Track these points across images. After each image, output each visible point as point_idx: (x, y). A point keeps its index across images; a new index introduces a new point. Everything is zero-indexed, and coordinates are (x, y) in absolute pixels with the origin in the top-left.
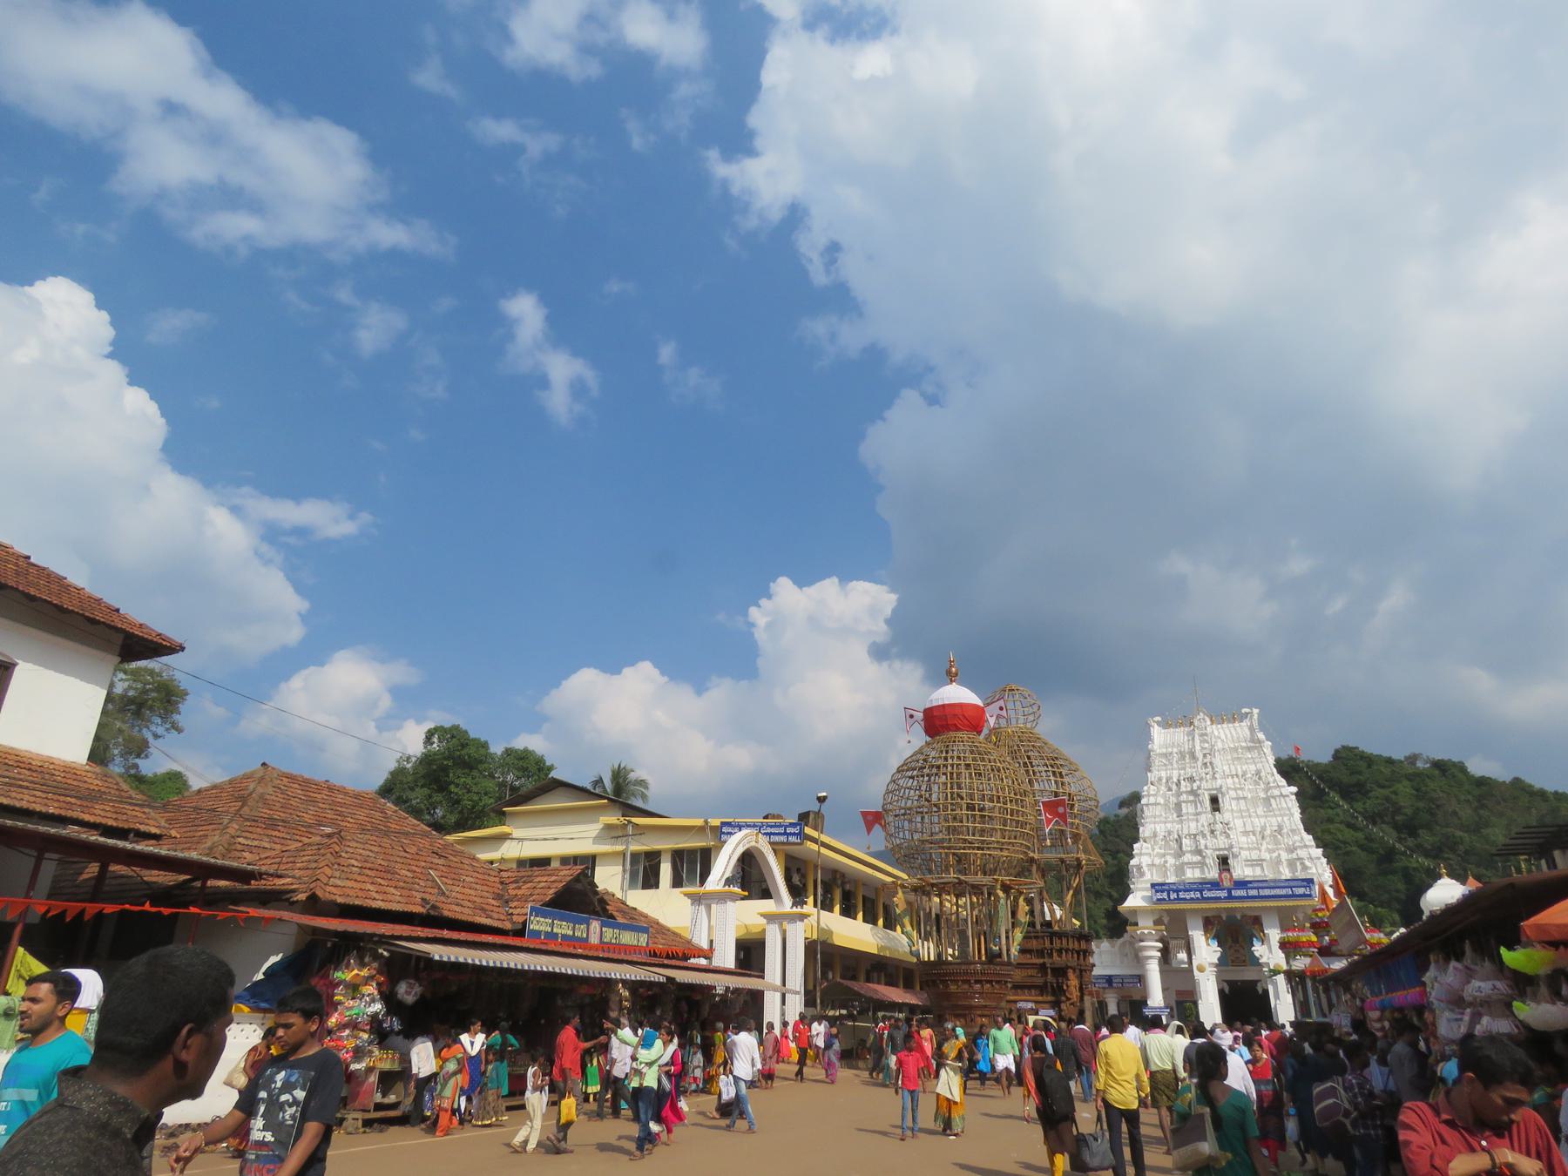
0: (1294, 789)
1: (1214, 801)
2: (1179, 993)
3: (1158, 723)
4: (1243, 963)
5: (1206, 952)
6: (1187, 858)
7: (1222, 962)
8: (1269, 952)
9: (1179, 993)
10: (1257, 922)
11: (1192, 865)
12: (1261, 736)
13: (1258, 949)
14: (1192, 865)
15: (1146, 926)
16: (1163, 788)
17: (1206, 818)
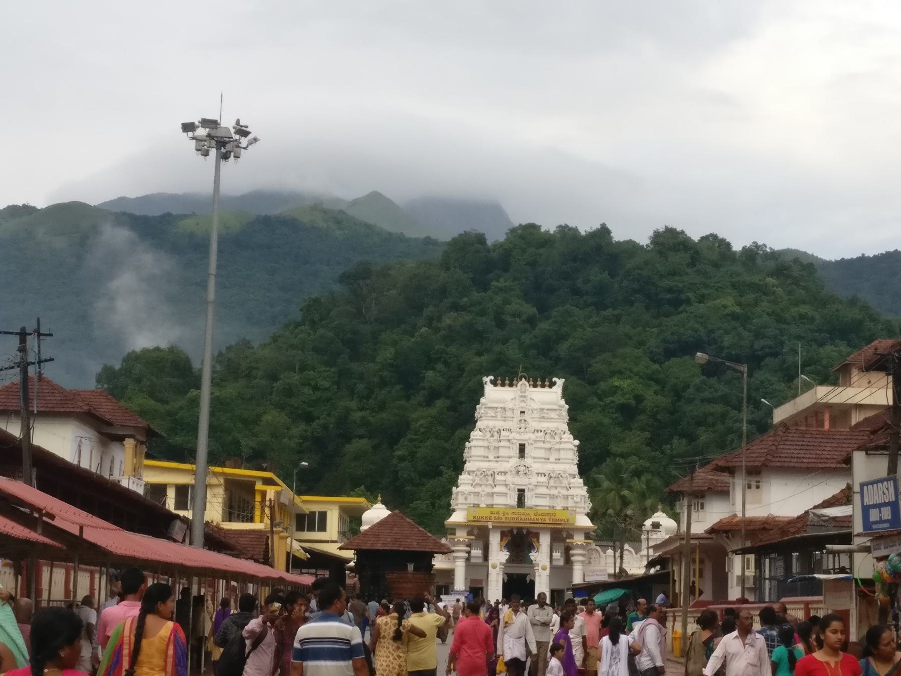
0: (577, 442)
1: (522, 449)
2: (472, 581)
3: (492, 382)
4: (521, 562)
5: (499, 556)
6: (498, 489)
7: (509, 561)
8: (542, 557)
9: (472, 581)
10: (537, 535)
11: (500, 494)
12: (563, 402)
13: (533, 555)
14: (500, 494)
15: (461, 535)
16: (489, 435)
17: (515, 461)
